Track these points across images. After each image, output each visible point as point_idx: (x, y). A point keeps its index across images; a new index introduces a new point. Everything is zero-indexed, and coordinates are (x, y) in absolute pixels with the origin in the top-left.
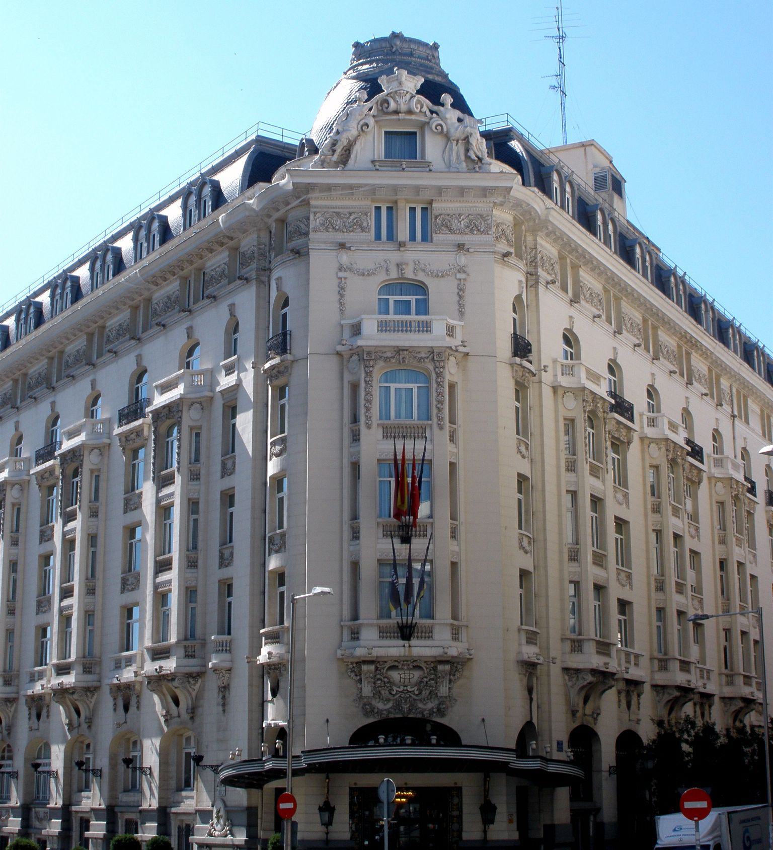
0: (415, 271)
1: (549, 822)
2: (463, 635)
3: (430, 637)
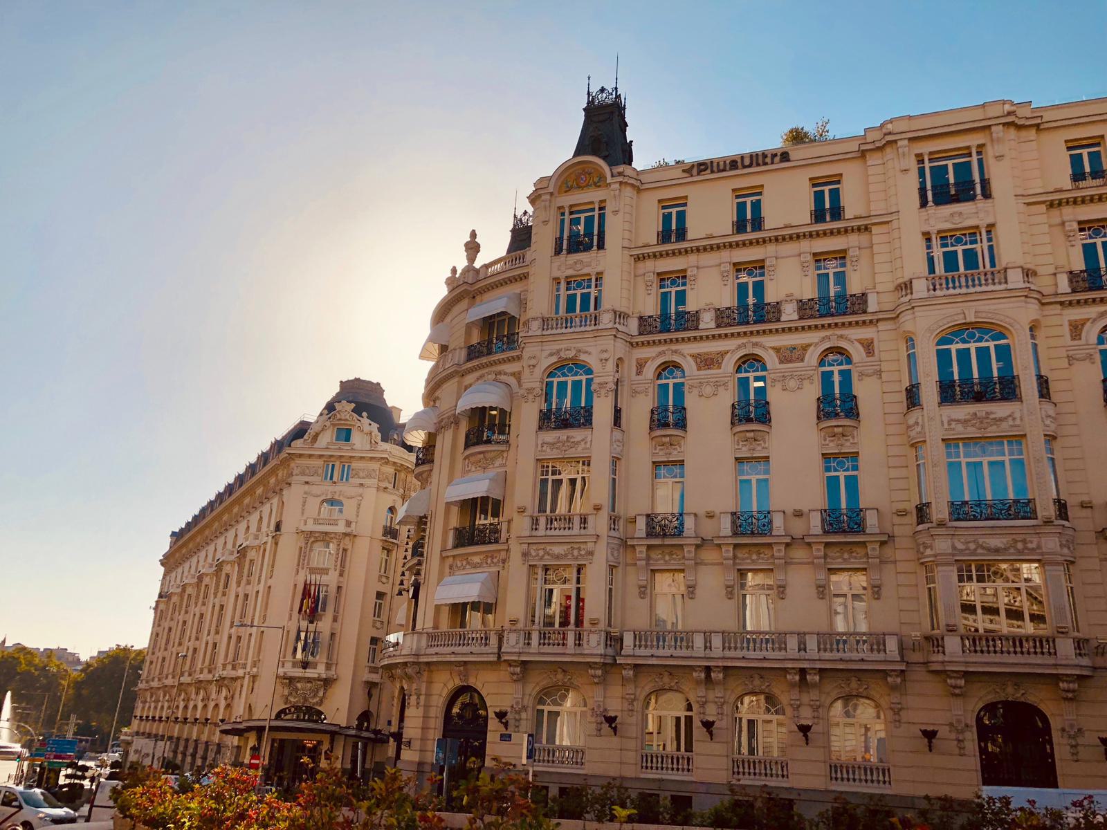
0: (340, 495)
3: (315, 668)
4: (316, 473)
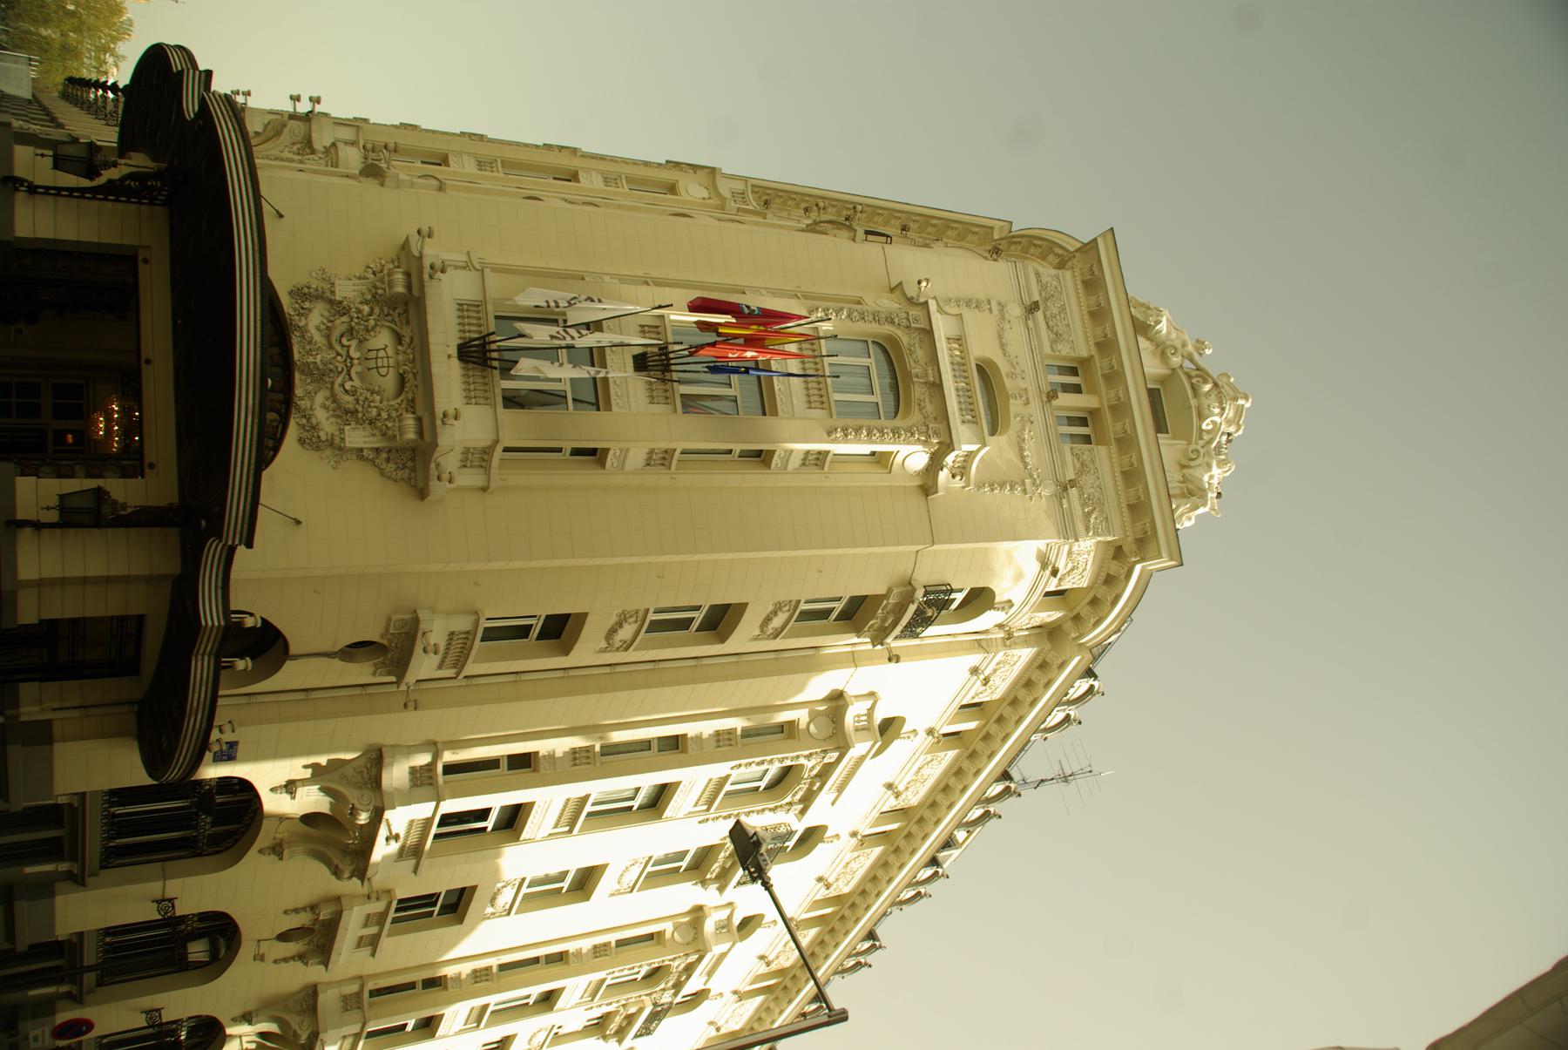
2: (472, 478)
4: (1057, 337)
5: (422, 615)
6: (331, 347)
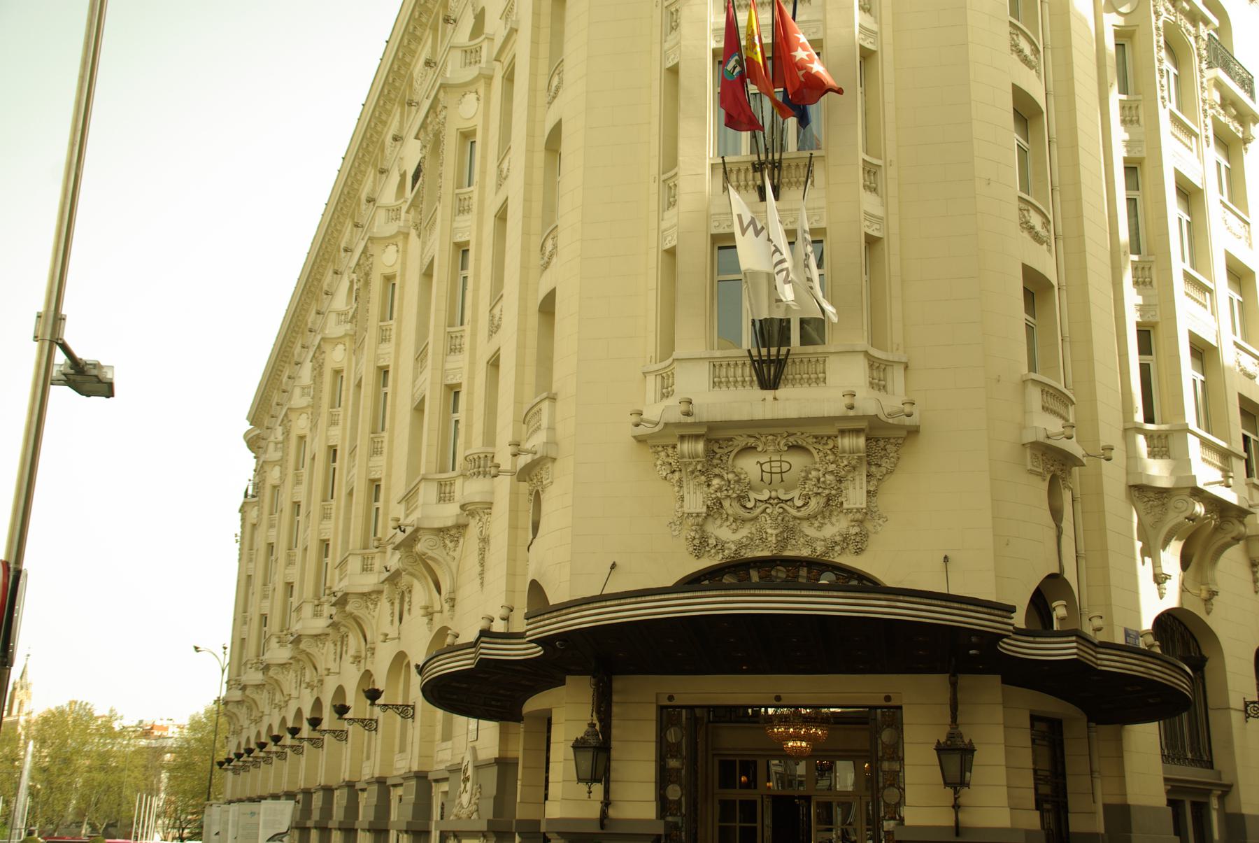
1: (1115, 800)
2: (896, 379)
5: (1029, 438)
6: (756, 518)
